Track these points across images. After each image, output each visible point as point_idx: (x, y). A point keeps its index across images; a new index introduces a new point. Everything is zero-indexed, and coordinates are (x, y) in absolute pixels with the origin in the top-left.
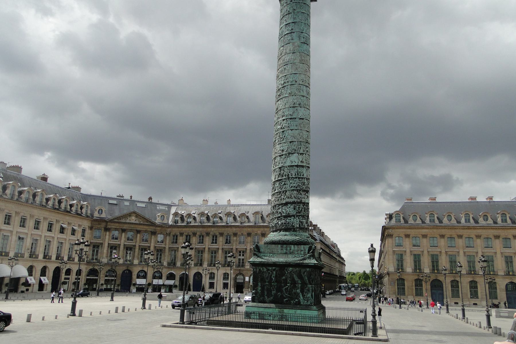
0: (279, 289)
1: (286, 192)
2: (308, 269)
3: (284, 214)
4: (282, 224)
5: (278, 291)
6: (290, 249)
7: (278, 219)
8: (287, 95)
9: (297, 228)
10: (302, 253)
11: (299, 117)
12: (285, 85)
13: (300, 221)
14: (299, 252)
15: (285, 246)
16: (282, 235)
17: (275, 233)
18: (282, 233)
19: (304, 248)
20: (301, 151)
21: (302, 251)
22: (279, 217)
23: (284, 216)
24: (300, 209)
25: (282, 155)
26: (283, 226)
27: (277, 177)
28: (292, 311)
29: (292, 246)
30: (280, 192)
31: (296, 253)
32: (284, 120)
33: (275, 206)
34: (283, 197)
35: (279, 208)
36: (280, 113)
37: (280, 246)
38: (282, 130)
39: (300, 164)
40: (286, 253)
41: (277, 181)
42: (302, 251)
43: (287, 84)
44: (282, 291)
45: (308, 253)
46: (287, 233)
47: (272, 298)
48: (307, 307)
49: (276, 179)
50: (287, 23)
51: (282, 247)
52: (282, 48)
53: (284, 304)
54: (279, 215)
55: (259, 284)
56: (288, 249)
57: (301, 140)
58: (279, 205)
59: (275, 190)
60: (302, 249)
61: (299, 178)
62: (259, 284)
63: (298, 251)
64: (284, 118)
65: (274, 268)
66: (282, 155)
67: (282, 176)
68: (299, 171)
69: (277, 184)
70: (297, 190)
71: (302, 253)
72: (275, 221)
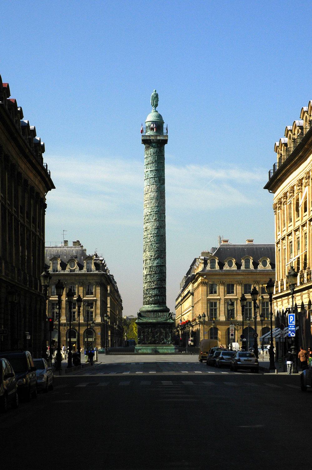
0: (153, 337)
1: (154, 281)
2: (169, 325)
3: (153, 295)
4: (152, 300)
5: (152, 338)
6: (159, 315)
7: (150, 298)
8: (153, 220)
9: (161, 302)
10: (165, 316)
11: (161, 235)
12: (151, 213)
13: (162, 298)
14: (164, 316)
15: (155, 313)
16: (153, 307)
17: (148, 305)
18: (152, 305)
19: (166, 314)
20: (162, 257)
21: (165, 315)
22: (151, 296)
23: (153, 296)
24: (163, 291)
25: (151, 259)
26: (153, 302)
27: (148, 272)
28: (160, 347)
29: (160, 313)
30: (151, 281)
31: (162, 317)
32: (151, 236)
33: (148, 289)
34: (152, 284)
35: (150, 291)
36: (149, 231)
37: (152, 313)
38: (151, 243)
39: (162, 264)
40: (156, 317)
41: (148, 274)
42: (165, 315)
43: (153, 213)
44: (154, 338)
45: (169, 316)
46: (156, 306)
47: (149, 342)
48: (169, 345)
49: (148, 273)
50: (151, 170)
51: (154, 314)
52: (148, 187)
53: (156, 344)
54: (151, 295)
55: (142, 334)
56: (157, 314)
57: (162, 249)
58: (150, 289)
59: (147, 280)
60: (165, 314)
61: (161, 273)
62: (142, 334)
63: (163, 315)
64: (151, 235)
65: (150, 325)
66: (151, 259)
67: (152, 272)
68: (161, 268)
69: (148, 277)
70: (161, 280)
71: (165, 316)
72: (148, 299)
